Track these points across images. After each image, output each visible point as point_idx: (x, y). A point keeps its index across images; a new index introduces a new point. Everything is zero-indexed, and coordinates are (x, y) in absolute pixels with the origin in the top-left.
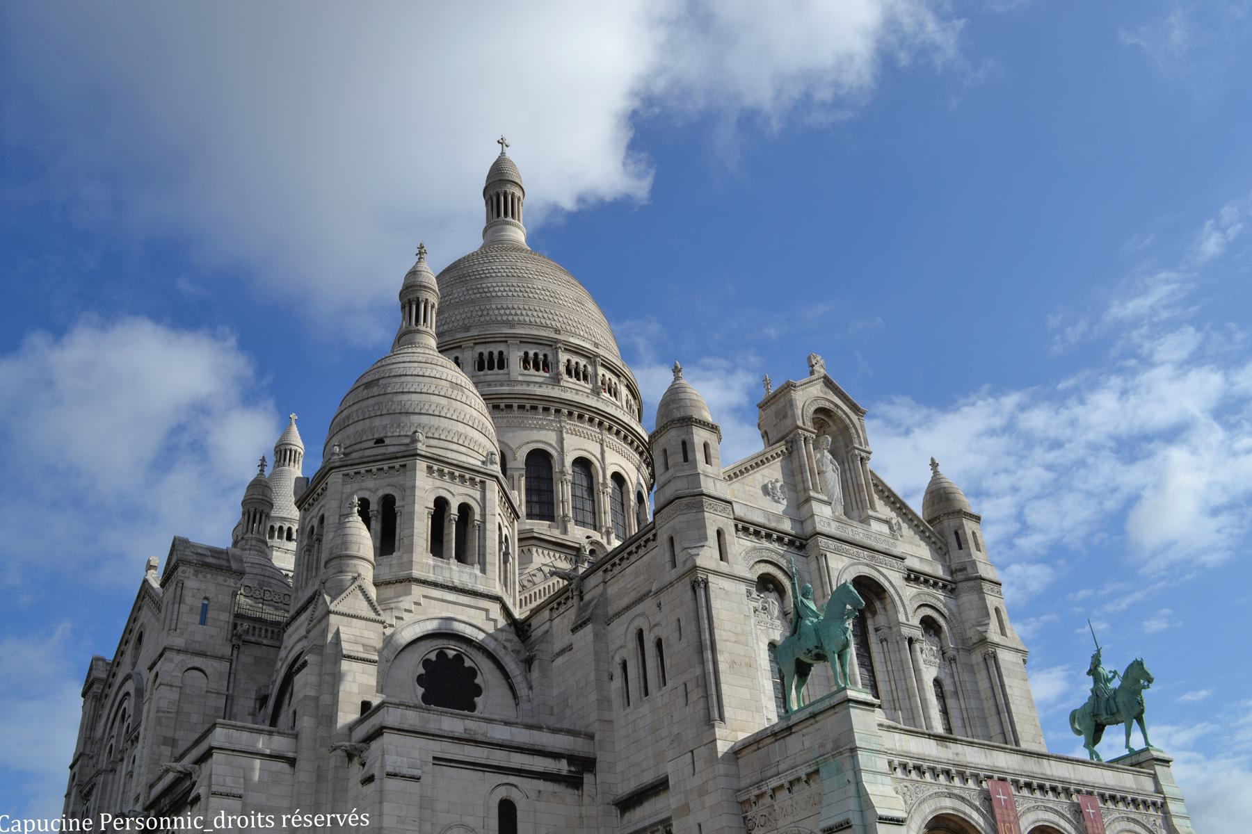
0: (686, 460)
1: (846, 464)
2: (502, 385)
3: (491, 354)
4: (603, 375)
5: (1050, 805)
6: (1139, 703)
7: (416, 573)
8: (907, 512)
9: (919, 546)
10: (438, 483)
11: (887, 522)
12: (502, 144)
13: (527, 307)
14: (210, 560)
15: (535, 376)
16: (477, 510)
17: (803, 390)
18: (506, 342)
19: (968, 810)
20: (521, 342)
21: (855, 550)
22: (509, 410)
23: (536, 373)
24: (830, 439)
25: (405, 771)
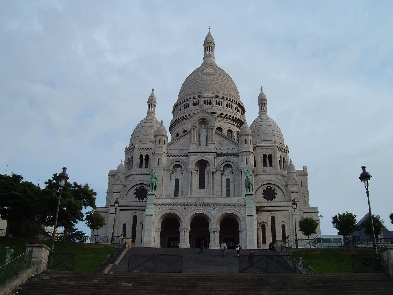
0: (155, 145)
3: (186, 104)
4: (217, 101)
7: (134, 173)
9: (230, 146)
10: (140, 152)
11: (215, 144)
12: (209, 29)
13: (196, 88)
17: (195, 116)
18: (189, 100)
19: (175, 211)
20: (192, 99)
22: (188, 119)
24: (203, 126)
25: (113, 213)
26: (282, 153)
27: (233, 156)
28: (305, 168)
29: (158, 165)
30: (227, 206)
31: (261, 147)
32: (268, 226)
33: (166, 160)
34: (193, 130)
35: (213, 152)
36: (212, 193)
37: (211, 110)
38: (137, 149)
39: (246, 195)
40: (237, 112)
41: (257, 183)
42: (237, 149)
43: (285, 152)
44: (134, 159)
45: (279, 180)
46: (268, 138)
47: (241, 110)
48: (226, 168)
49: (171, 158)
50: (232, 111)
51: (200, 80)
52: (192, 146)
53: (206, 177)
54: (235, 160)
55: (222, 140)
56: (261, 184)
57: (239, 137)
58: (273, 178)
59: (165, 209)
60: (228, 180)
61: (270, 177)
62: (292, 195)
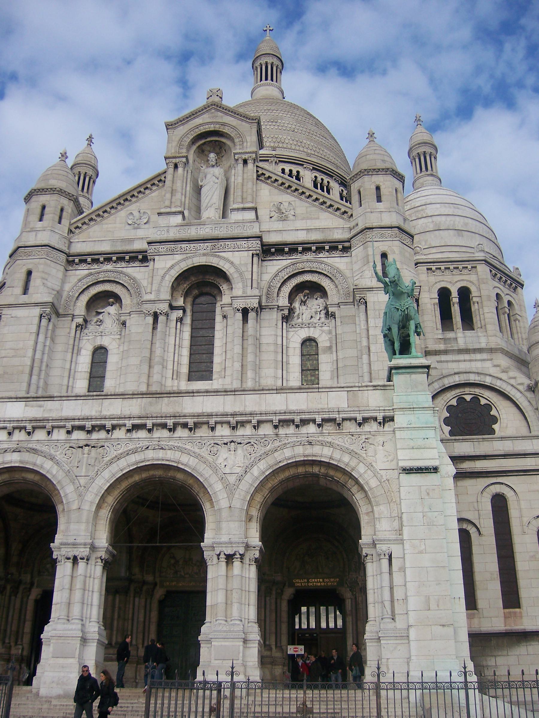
1: (233, 171)
4: (283, 171)
5: (170, 443)
6: (398, 309)
8: (305, 190)
17: (183, 124)
21: (192, 245)
24: (212, 155)
26: (502, 287)
27: (328, 252)
29: (25, 291)
30: (297, 426)
32: (480, 534)
33: (60, 275)
34: (171, 170)
35: (245, 234)
39: (393, 371)
45: (503, 372)
46: (450, 238)
48: (301, 296)
49: (82, 271)
52: (163, 221)
53: (218, 334)
54: (337, 265)
57: (351, 182)
58: (479, 365)
61: (470, 361)
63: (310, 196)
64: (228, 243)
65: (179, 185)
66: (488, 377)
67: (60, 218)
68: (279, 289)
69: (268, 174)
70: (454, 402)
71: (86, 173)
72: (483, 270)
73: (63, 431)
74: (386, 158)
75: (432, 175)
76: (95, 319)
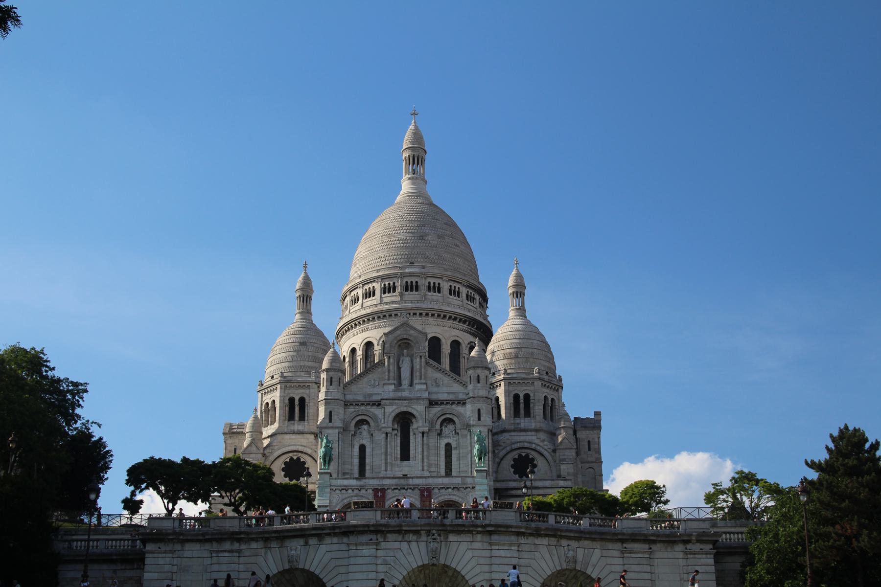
0: (323, 386)
1: (415, 361)
2: (370, 308)
3: (370, 288)
4: (429, 283)
9: (452, 386)
10: (290, 391)
11: (426, 384)
13: (388, 255)
14: (235, 430)
15: (388, 297)
16: (307, 399)
18: (375, 281)
20: (382, 279)
23: (390, 295)
24: (405, 351)
28: (598, 414)
29: (330, 421)
30: (446, 489)
31: (509, 381)
33: (343, 411)
35: (422, 398)
36: (420, 468)
37: (418, 302)
38: (283, 386)
40: (469, 303)
41: (502, 446)
42: (464, 391)
43: (555, 388)
44: (277, 404)
47: (477, 297)
48: (445, 424)
49: (351, 409)
50: (461, 303)
51: (397, 239)
52: (386, 387)
55: (438, 375)
56: (508, 449)
58: (530, 438)
59: (347, 496)
60: (448, 447)
62: (563, 467)
63: (449, 375)
64: (415, 401)
65: (391, 367)
66: (533, 445)
67: (339, 384)
68: (436, 421)
69: (431, 363)
70: (517, 457)
71: (307, 295)
72: (538, 384)
73: (371, 490)
74: (483, 359)
75: (520, 309)
76: (358, 432)
